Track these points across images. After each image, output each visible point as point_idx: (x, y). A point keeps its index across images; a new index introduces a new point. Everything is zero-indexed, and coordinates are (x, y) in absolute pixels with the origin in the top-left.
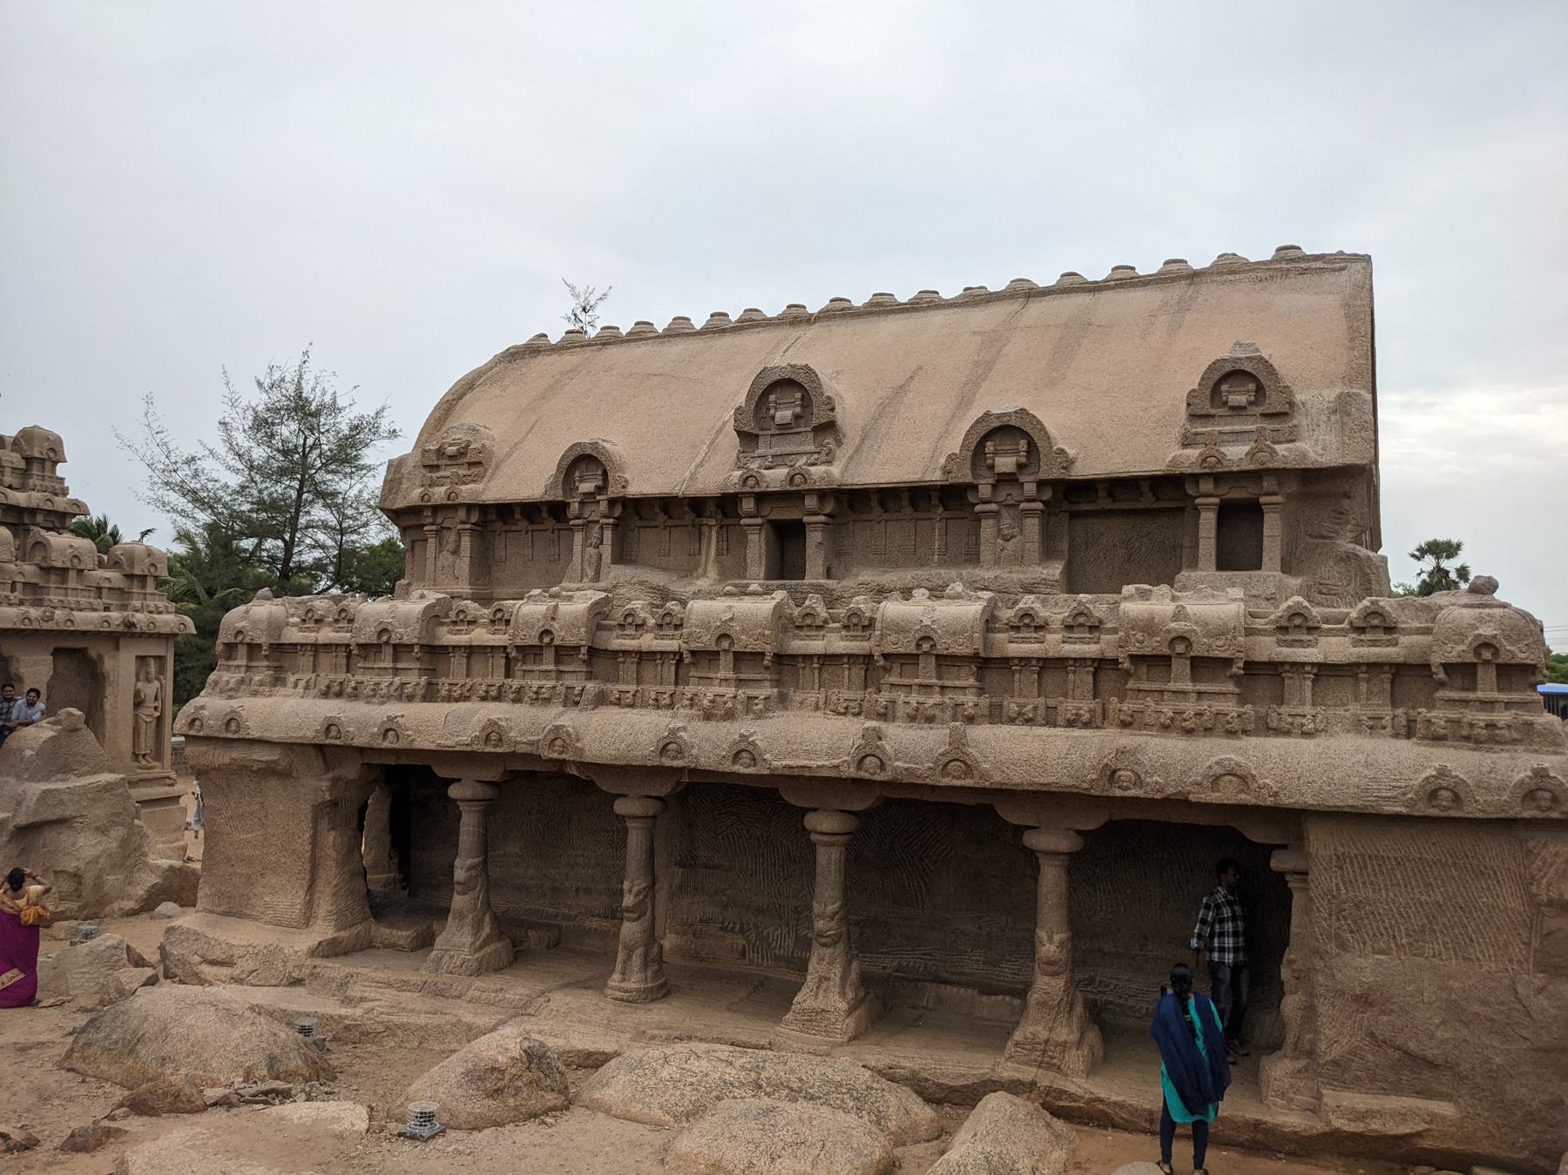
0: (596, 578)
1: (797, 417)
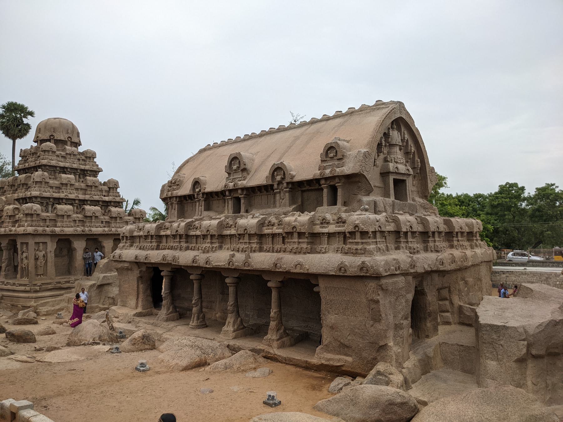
0: (201, 216)
1: (238, 167)
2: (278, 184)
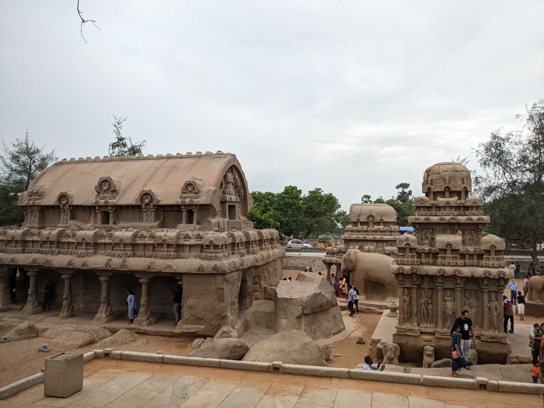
0: (66, 224)
1: (108, 188)
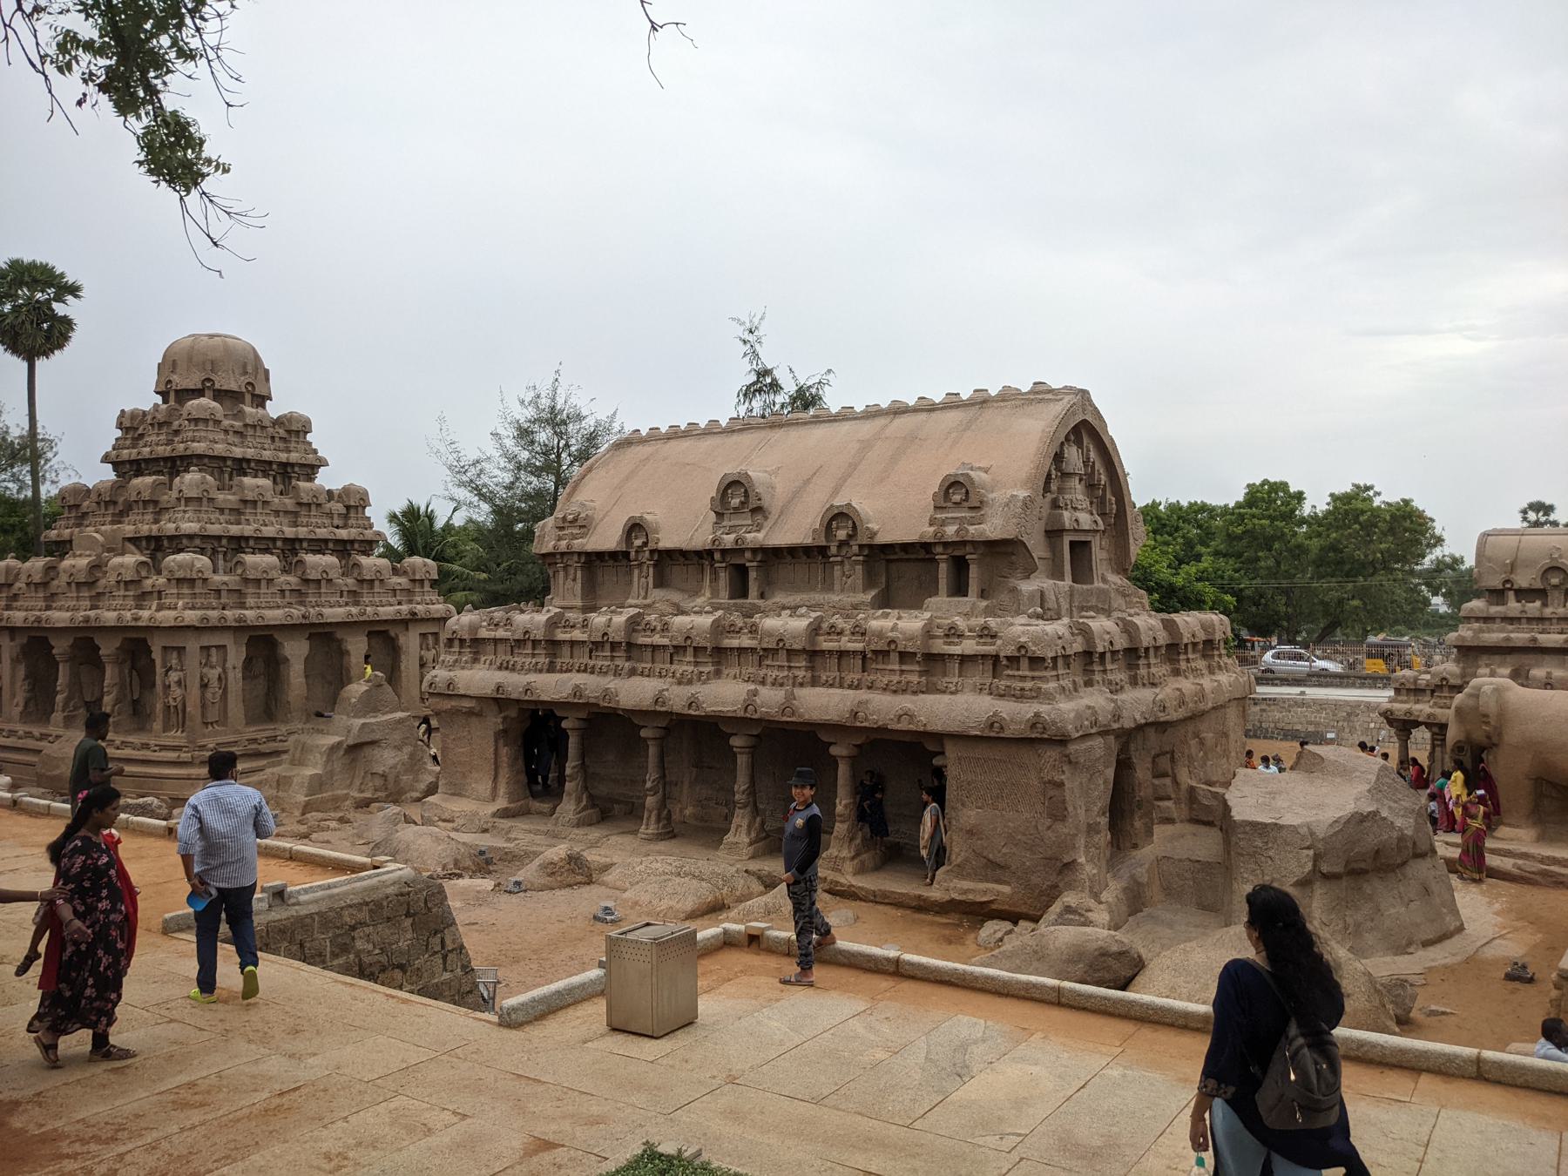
1: (742, 503)
2: (839, 547)
